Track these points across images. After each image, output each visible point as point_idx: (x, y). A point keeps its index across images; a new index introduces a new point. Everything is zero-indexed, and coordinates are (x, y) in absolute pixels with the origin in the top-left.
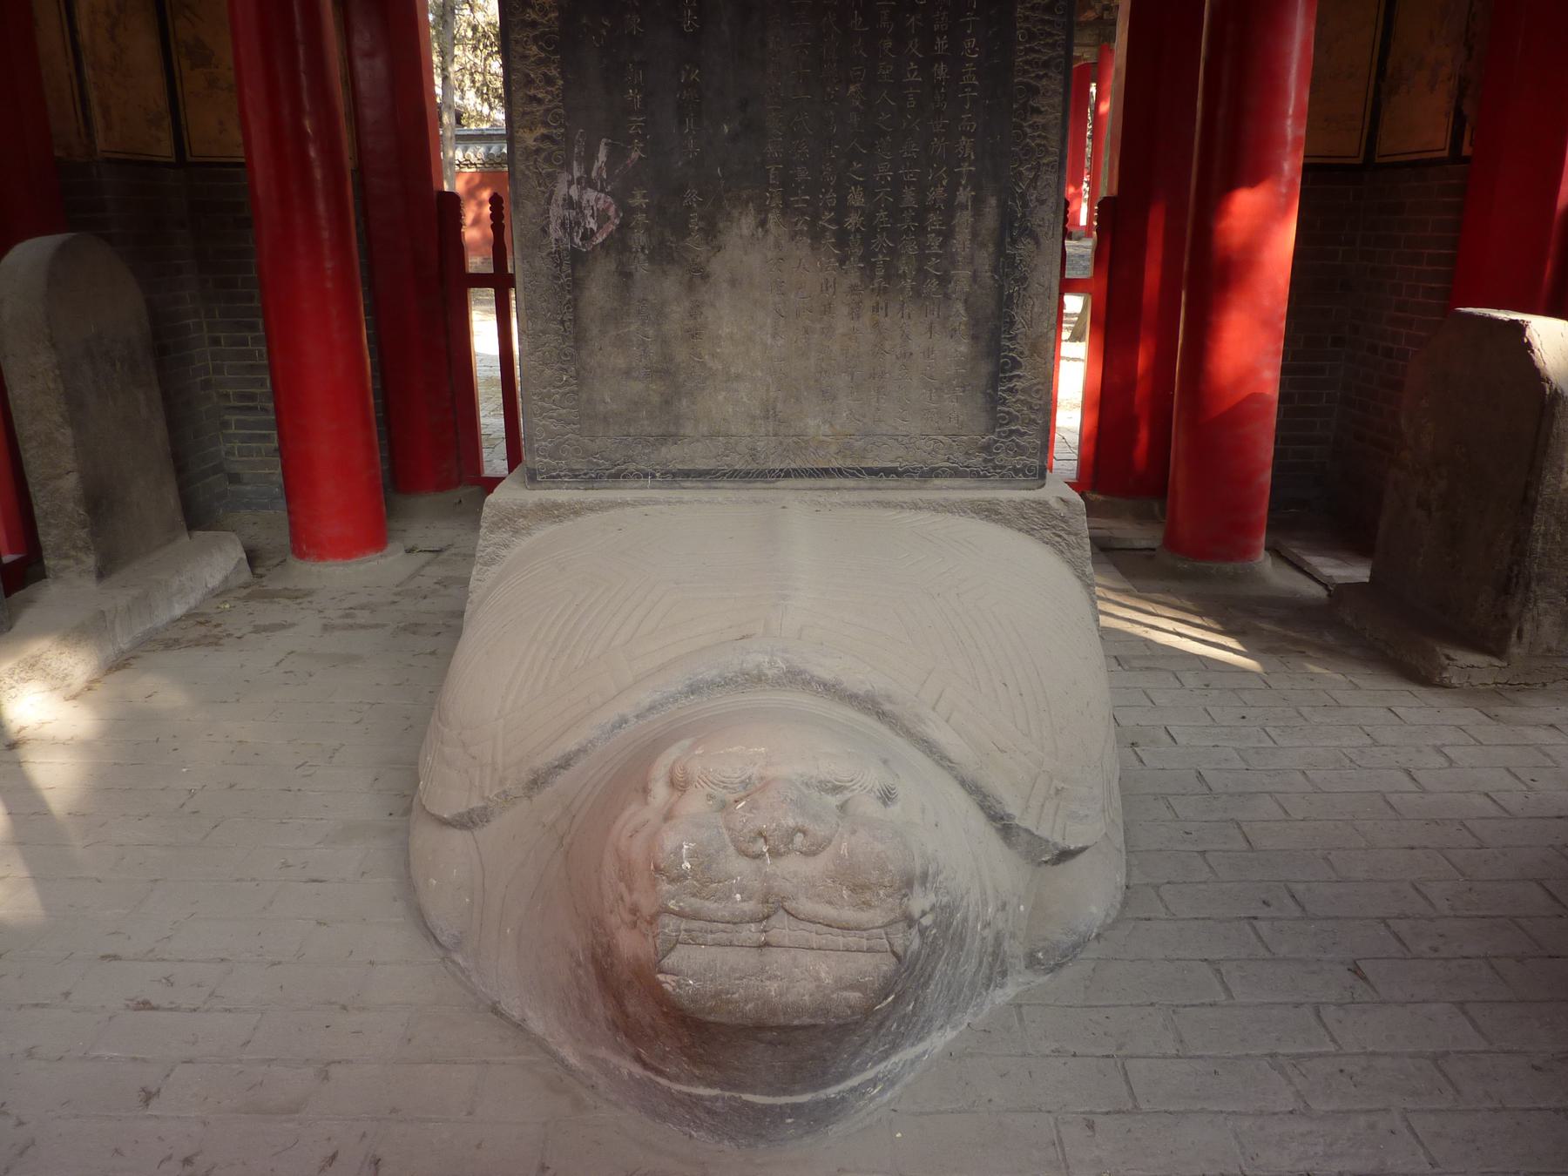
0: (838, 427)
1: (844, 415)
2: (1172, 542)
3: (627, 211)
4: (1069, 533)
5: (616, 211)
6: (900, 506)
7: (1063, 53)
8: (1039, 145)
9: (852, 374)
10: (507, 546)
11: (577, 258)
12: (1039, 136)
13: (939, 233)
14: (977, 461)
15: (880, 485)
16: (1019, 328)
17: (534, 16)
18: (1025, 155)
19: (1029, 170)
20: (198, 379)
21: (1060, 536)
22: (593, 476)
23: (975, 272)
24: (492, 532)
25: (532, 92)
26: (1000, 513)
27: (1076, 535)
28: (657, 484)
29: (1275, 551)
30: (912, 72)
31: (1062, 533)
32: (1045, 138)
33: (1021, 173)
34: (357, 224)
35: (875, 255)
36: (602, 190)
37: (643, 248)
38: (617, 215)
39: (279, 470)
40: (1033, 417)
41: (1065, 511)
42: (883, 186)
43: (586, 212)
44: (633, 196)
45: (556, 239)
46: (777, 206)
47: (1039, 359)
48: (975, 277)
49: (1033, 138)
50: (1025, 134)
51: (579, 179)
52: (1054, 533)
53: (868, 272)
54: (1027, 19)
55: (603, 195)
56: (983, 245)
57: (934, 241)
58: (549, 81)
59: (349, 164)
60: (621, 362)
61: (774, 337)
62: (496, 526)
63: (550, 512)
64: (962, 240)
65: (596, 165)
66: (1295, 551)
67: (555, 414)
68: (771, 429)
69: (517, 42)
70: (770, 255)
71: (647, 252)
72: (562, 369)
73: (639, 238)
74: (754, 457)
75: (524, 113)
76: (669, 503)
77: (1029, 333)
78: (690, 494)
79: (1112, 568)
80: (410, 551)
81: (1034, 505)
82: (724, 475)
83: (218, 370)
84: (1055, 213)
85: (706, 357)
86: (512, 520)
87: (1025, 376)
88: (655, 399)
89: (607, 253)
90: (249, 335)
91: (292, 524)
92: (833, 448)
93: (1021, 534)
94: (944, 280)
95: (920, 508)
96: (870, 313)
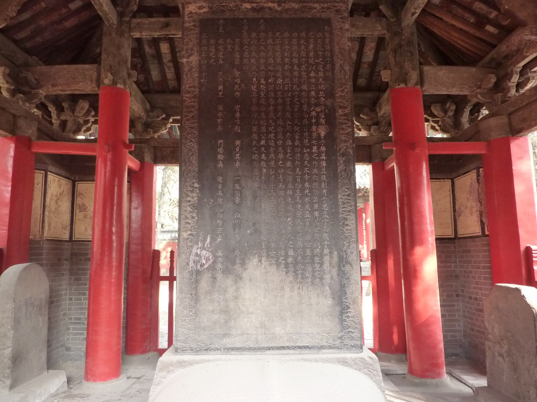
0: (287, 331)
1: (289, 326)
2: (411, 371)
3: (216, 257)
4: (374, 370)
5: (212, 257)
6: (311, 360)
7: (354, 208)
8: (349, 235)
10: (165, 378)
11: (198, 273)
12: (349, 233)
13: (319, 263)
14: (338, 343)
15: (303, 352)
16: (348, 295)
17: (190, 199)
18: (345, 238)
20: (62, 313)
21: (370, 371)
22: (199, 350)
23: (332, 276)
24: (160, 372)
25: (187, 221)
26: (348, 363)
27: (376, 371)
28: (222, 353)
29: (450, 374)
30: (307, 214)
31: (371, 370)
32: (351, 233)
34: (125, 260)
35: (298, 271)
36: (208, 251)
37: (220, 269)
39: (85, 346)
40: (356, 326)
41: (371, 361)
42: (300, 249)
43: (202, 258)
44: (218, 253)
45: (191, 267)
46: (265, 256)
47: (356, 305)
48: (332, 278)
49: (347, 233)
50: (344, 232)
52: (368, 370)
53: (296, 276)
54: (342, 198)
56: (333, 267)
57: (317, 266)
58: (193, 217)
59: (125, 240)
60: (211, 308)
61: (264, 299)
62: (161, 370)
63: (181, 364)
65: (206, 243)
66: (457, 374)
67: (186, 327)
68: (263, 332)
69: (184, 206)
70: (263, 271)
71: (222, 270)
73: (219, 266)
74: (257, 342)
75: (184, 227)
76: (226, 360)
78: (234, 357)
79: (391, 382)
80: (128, 378)
81: (359, 359)
82: (246, 349)
83: (70, 309)
84: (356, 256)
85: (241, 306)
86: (168, 367)
87: (352, 312)
88: (222, 321)
89: (208, 271)
90: (83, 297)
91: (86, 367)
92: (286, 339)
93: (356, 371)
94: (321, 279)
95: (318, 361)
96: (297, 290)
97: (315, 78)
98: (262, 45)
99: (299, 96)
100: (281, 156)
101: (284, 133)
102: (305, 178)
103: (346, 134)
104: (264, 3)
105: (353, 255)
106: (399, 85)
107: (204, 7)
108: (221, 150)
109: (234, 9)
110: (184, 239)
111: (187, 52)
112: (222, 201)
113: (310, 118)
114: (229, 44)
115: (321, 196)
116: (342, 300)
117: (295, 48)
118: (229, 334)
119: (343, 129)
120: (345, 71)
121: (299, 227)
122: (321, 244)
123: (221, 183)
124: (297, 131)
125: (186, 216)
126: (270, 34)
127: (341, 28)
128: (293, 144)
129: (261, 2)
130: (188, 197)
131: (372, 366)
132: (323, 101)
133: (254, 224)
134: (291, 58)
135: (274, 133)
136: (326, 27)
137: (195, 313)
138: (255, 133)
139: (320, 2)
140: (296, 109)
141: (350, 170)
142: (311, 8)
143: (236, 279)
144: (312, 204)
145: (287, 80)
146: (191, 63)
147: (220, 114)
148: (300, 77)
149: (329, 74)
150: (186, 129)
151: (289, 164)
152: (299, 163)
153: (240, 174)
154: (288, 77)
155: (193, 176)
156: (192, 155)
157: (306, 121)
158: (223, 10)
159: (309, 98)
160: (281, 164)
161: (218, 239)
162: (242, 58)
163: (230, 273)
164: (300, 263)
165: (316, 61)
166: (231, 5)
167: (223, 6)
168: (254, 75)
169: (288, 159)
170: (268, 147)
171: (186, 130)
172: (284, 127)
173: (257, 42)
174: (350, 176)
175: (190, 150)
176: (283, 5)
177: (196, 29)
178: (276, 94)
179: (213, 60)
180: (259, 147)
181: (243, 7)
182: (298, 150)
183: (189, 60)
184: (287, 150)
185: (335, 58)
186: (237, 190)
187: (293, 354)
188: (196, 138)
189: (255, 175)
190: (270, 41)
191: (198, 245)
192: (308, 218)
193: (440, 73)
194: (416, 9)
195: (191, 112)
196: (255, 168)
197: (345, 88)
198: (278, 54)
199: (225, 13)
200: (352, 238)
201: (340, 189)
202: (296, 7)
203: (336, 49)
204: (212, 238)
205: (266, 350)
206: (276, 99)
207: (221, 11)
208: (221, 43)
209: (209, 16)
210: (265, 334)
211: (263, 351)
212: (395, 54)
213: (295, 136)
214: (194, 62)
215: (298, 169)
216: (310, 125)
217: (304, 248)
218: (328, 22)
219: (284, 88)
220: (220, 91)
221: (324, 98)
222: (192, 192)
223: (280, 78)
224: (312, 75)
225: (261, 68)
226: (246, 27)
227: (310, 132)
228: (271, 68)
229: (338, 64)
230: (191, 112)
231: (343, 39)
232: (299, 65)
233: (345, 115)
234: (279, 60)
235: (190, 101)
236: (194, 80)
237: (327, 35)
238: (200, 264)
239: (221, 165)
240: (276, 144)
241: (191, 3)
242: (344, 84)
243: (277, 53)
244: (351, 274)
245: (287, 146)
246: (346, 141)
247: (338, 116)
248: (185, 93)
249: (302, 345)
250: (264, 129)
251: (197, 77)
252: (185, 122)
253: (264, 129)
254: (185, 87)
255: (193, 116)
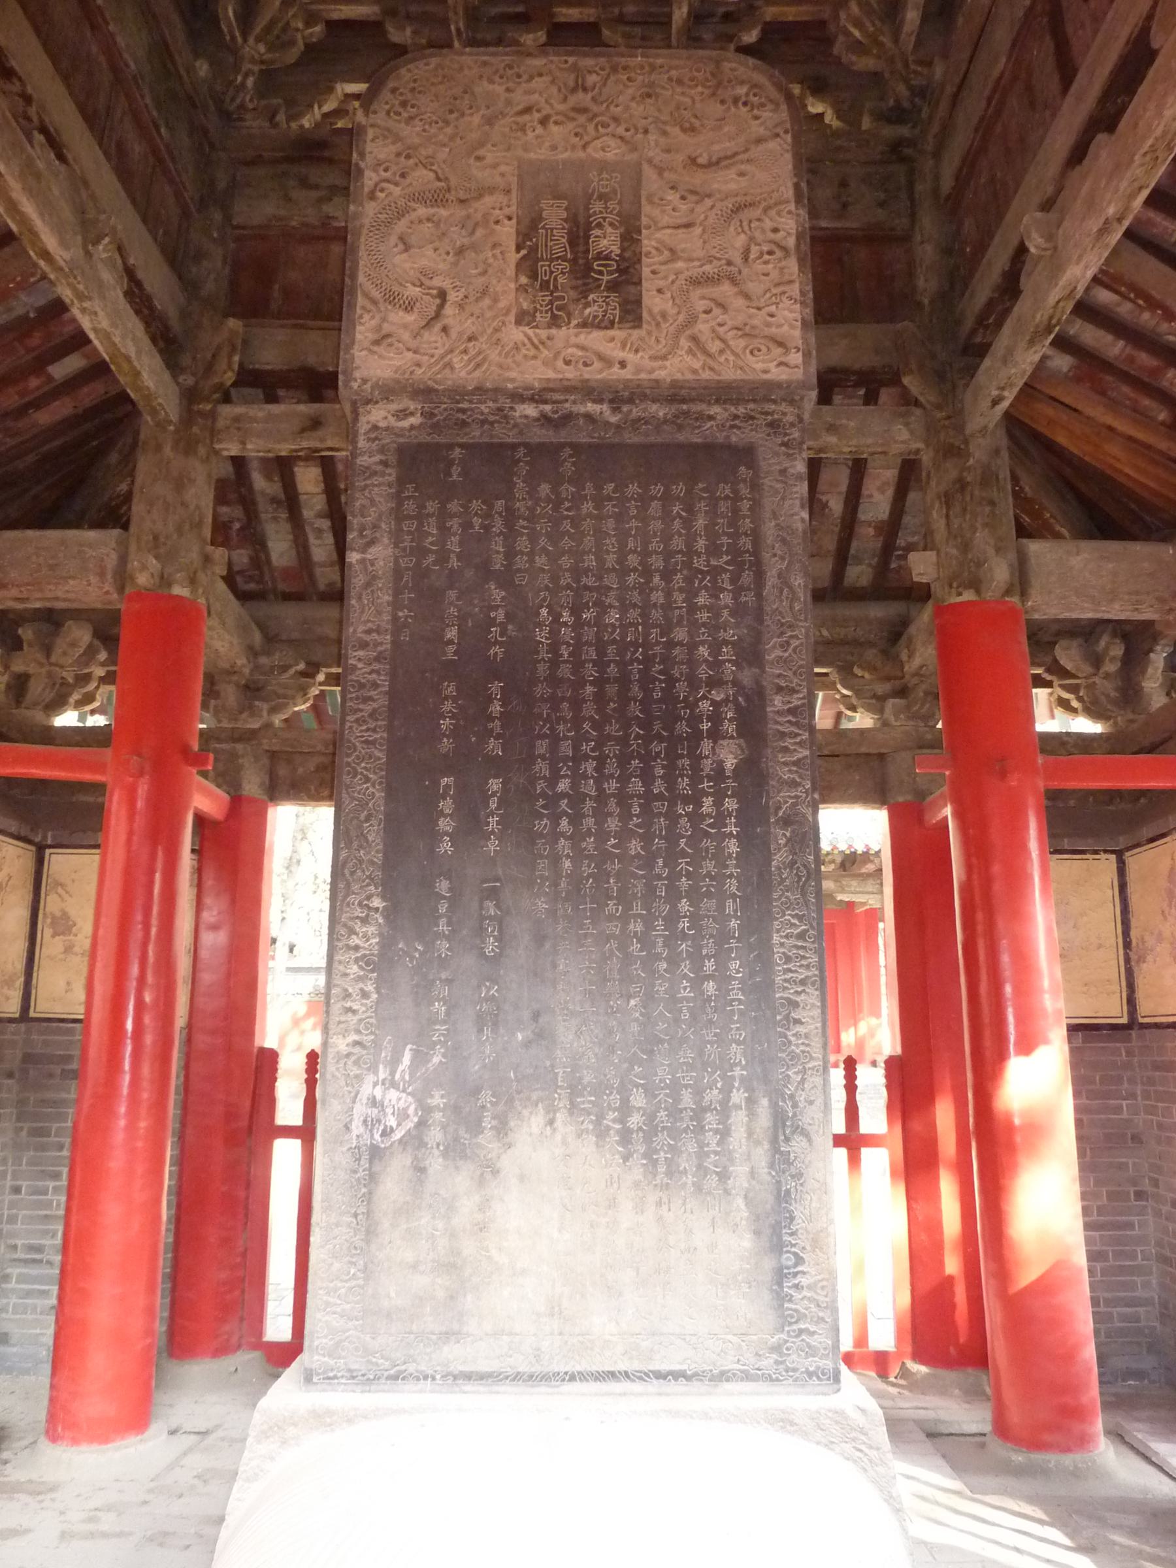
2: (1002, 1429)
3: (426, 1110)
4: (871, 1447)
5: (416, 1110)
8: (803, 1052)
9: (638, 1270)
10: (272, 1459)
13: (716, 1131)
14: (768, 1362)
16: (798, 1224)
19: (796, 1073)
21: (861, 1451)
25: (348, 1004)
27: (878, 1449)
29: (1118, 1436)
30: (685, 988)
31: (863, 1447)
32: (808, 1045)
33: (788, 1076)
34: (178, 1077)
35: (656, 1151)
36: (404, 1091)
37: (438, 1145)
38: (416, 1114)
39: (51, 1331)
40: (821, 1314)
42: (662, 1089)
44: (432, 1097)
45: (358, 1136)
48: (752, 1174)
50: (790, 1042)
51: (384, 1080)
54: (782, 944)
55: (404, 1095)
56: (758, 1143)
57: (712, 1140)
58: (365, 995)
60: (409, 1256)
63: (321, 1419)
64: (738, 1138)
65: (401, 1068)
66: (1140, 1436)
67: (338, 1310)
69: (340, 962)
72: (351, 1263)
73: (435, 1135)
75: (340, 1022)
77: (809, 1228)
78: (473, 1399)
79: (941, 1462)
80: (172, 1432)
81: (830, 1414)
82: (507, 1378)
87: (810, 1274)
88: (441, 1294)
90: (51, 1184)
91: (52, 1400)
94: (724, 1176)
96: (653, 1208)
97: (709, 609)
98: (567, 517)
99: (666, 659)
100: (613, 824)
101: (623, 760)
102: (678, 887)
103: (795, 763)
104: (574, 402)
105: (813, 1107)
106: (960, 594)
107: (412, 414)
108: (447, 805)
109: (491, 418)
110: (339, 1057)
111: (361, 535)
112: (448, 949)
113: (695, 720)
114: (476, 514)
115: (723, 937)
116: (780, 1237)
117: (656, 525)
118: (459, 1333)
119: (785, 750)
120: (791, 588)
121: (662, 1026)
122: (723, 1077)
123: (445, 898)
124: (658, 754)
125: (346, 990)
126: (589, 489)
127: (783, 472)
128: (648, 791)
129: (567, 401)
130: (354, 937)
131: (865, 1434)
132: (733, 671)
133: (536, 1016)
134: (645, 554)
135: (594, 759)
136: (743, 469)
137: (365, 1270)
138: (543, 758)
139: (725, 402)
140: (657, 695)
141: (805, 866)
142: (702, 417)
143: (482, 1174)
144: (697, 959)
145: (633, 614)
146: (372, 565)
147: (448, 706)
148: (668, 606)
149: (748, 598)
150: (354, 745)
151: (635, 846)
152: (663, 844)
153: (500, 872)
154: (635, 606)
155: (369, 877)
156: (367, 819)
157: (682, 728)
158: (463, 420)
159: (692, 662)
160: (613, 846)
161: (432, 1056)
162: (510, 554)
163: (464, 1157)
164: (662, 1131)
165: (713, 562)
166: (483, 407)
167: (463, 411)
168: (544, 600)
169: (633, 833)
170: (577, 799)
171: (355, 750)
172: (624, 741)
173: (553, 509)
174: (807, 880)
175: (363, 805)
176: (625, 409)
177: (388, 471)
178: (601, 652)
179: (431, 558)
180: (553, 800)
181: (517, 414)
182: (660, 807)
183: (368, 556)
184: (631, 806)
185: (766, 556)
186: (490, 918)
187: (641, 1394)
188: (381, 770)
189: (541, 877)
190: (587, 507)
191: (376, 1073)
192: (687, 999)
193: (1076, 561)
194: (1003, 389)
195: (371, 699)
196: (541, 857)
197: (791, 637)
198: (611, 543)
199: (468, 430)
200: (812, 1058)
201: (777, 919)
202: (661, 414)
203: (769, 530)
204: (416, 1054)
205: (563, 1380)
206: (601, 664)
207: (456, 424)
208: (455, 510)
209: (424, 438)
210: (561, 1334)
211: (553, 1383)
212: (948, 508)
213: (654, 767)
214: (381, 563)
215: (660, 862)
216: (696, 737)
217: (675, 1088)
218: (747, 454)
219: (623, 635)
220: (451, 642)
221: (734, 663)
222: (365, 921)
223: (615, 607)
224: (701, 600)
225: (563, 582)
226: (523, 469)
227: (697, 759)
228: (590, 581)
229: (774, 572)
230: (371, 699)
231: (788, 503)
232: (667, 575)
233: (792, 711)
234: (611, 560)
235: (368, 670)
236: (379, 613)
237: (744, 490)
238: (381, 1128)
239: (446, 846)
240: (600, 790)
241: (377, 402)
242: (790, 626)
243: (608, 541)
244: (807, 1162)
245: (632, 797)
246: (794, 784)
247: (771, 715)
248: (354, 646)
249: (664, 1367)
250: (566, 748)
251: (388, 603)
252: (351, 727)
253: (566, 748)
254: (355, 631)
255: (375, 710)
